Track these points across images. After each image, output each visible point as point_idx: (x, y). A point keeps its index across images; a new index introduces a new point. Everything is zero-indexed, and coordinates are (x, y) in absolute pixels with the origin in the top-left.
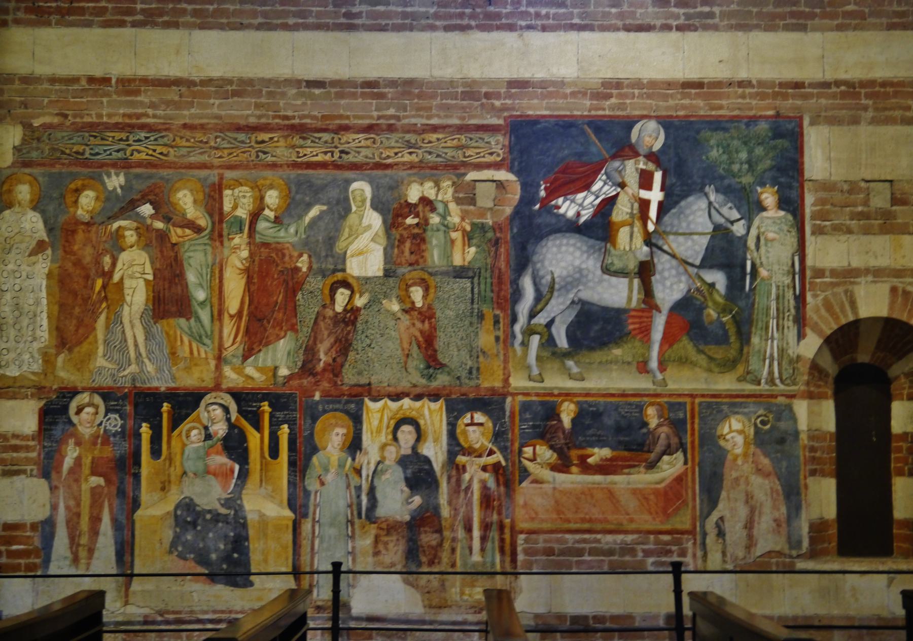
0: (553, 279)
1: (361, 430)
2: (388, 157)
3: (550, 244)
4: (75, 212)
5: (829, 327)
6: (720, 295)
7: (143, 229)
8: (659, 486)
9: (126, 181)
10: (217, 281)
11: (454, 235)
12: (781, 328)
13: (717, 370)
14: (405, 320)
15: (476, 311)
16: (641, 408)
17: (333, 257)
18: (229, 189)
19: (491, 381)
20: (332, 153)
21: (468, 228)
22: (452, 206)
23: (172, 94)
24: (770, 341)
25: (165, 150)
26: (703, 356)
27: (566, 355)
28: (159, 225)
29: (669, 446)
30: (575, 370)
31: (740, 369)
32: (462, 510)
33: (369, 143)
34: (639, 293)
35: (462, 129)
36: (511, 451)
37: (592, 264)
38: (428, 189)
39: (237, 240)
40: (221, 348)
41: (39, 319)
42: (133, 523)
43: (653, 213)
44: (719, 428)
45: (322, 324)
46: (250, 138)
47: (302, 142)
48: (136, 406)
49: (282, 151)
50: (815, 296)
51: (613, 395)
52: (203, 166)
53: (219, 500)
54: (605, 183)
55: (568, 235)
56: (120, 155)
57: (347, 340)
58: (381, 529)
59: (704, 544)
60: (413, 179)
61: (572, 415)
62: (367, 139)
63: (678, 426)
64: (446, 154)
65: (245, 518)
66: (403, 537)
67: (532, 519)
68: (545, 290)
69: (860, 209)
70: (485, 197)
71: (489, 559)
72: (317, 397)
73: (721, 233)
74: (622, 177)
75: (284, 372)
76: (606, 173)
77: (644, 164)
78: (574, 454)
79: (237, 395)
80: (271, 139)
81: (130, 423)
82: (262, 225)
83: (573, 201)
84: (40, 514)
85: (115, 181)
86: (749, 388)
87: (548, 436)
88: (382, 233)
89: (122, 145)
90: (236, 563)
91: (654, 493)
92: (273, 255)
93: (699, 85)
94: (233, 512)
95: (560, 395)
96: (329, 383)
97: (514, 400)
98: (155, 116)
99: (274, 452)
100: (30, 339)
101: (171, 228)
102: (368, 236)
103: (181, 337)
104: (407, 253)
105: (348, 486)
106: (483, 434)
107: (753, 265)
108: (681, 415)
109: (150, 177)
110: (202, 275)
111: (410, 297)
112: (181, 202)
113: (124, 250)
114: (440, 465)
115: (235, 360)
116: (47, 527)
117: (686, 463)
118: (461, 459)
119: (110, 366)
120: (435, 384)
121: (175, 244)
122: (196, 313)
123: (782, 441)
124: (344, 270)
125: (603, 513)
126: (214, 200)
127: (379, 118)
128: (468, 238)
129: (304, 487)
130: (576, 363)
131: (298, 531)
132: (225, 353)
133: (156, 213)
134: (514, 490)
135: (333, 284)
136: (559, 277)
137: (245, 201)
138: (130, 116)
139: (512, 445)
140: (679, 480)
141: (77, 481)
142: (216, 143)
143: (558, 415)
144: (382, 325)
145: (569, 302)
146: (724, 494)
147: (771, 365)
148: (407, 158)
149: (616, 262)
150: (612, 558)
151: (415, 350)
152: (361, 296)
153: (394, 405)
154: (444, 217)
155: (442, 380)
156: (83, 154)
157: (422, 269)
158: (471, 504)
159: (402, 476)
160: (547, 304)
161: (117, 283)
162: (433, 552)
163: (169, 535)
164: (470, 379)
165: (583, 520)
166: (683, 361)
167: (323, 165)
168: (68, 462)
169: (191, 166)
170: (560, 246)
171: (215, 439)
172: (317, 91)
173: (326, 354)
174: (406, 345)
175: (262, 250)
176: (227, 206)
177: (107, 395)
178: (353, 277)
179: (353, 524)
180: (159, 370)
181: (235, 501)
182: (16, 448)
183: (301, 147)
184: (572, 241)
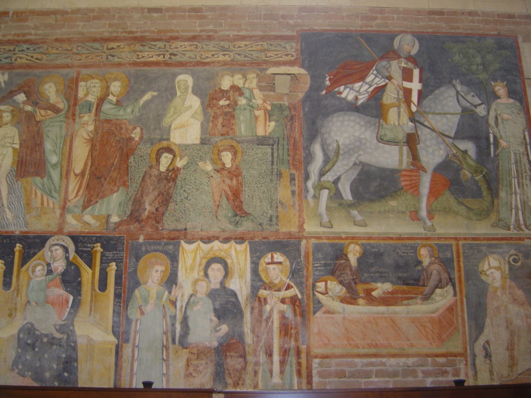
0: (338, 146)
1: (177, 267)
2: (207, 57)
3: (335, 119)
6: (472, 160)
7: (17, 112)
8: (433, 315)
9: (9, 78)
10: (68, 148)
11: (257, 113)
12: (521, 185)
14: (217, 177)
15: (276, 170)
16: (415, 249)
18: (84, 81)
20: (164, 55)
21: (269, 108)
23: (51, 20)
24: (514, 195)
26: (463, 207)
27: (351, 205)
28: (29, 108)
29: (440, 281)
30: (359, 218)
31: (493, 217)
32: (264, 337)
33: (192, 48)
34: (408, 158)
35: (263, 38)
36: (306, 286)
39: (86, 118)
40: (66, 200)
43: (415, 98)
44: (481, 265)
45: (148, 181)
46: (103, 47)
47: (141, 48)
51: (391, 239)
52: (67, 66)
54: (376, 76)
55: (349, 113)
56: (7, 61)
57: (168, 194)
58: (192, 353)
59: (474, 365)
60: (225, 72)
62: (191, 45)
64: (252, 55)
65: (75, 342)
66: (211, 361)
67: (325, 345)
68: (332, 154)
72: (141, 239)
74: (389, 72)
75: (115, 219)
76: (376, 69)
77: (405, 64)
78: (360, 288)
79: (75, 238)
80: (118, 46)
82: (106, 107)
83: (352, 89)
86: (501, 232)
87: (338, 273)
88: (200, 111)
91: (430, 321)
92: (114, 129)
93: (441, 13)
94: (65, 337)
95: (347, 238)
96: (152, 228)
97: (308, 242)
98: (36, 35)
99: (103, 286)
101: (37, 110)
102: (188, 114)
103: (36, 191)
104: (219, 126)
105: (165, 316)
106: (282, 271)
107: (495, 138)
108: (449, 255)
110: (56, 144)
111: (221, 160)
112: (47, 92)
115: (76, 210)
117: (455, 295)
118: (263, 293)
120: (241, 229)
121: (39, 122)
122: (49, 173)
124: (168, 139)
125: (387, 339)
126: (72, 89)
127: (201, 31)
128: (269, 115)
129: (127, 316)
130: (359, 212)
134: (309, 320)
137: (95, 90)
138: (18, 35)
139: (307, 280)
140: (451, 309)
142: (77, 50)
143: (346, 255)
144: (197, 182)
145: (351, 164)
146: (488, 321)
147: (517, 214)
148: (221, 58)
149: (388, 133)
150: (396, 379)
152: (181, 159)
153: (205, 247)
154: (250, 100)
155: (246, 226)
157: (232, 139)
158: (272, 332)
159: (211, 307)
160: (334, 165)
162: (238, 374)
163: (12, 354)
164: (270, 225)
165: (370, 346)
166: (447, 211)
167: (157, 64)
169: (57, 67)
171: (55, 274)
172: (155, 15)
173: (150, 205)
174: (217, 198)
175: (105, 125)
178: (175, 144)
179: (167, 349)
181: (68, 327)
183: (141, 52)
184: (352, 118)
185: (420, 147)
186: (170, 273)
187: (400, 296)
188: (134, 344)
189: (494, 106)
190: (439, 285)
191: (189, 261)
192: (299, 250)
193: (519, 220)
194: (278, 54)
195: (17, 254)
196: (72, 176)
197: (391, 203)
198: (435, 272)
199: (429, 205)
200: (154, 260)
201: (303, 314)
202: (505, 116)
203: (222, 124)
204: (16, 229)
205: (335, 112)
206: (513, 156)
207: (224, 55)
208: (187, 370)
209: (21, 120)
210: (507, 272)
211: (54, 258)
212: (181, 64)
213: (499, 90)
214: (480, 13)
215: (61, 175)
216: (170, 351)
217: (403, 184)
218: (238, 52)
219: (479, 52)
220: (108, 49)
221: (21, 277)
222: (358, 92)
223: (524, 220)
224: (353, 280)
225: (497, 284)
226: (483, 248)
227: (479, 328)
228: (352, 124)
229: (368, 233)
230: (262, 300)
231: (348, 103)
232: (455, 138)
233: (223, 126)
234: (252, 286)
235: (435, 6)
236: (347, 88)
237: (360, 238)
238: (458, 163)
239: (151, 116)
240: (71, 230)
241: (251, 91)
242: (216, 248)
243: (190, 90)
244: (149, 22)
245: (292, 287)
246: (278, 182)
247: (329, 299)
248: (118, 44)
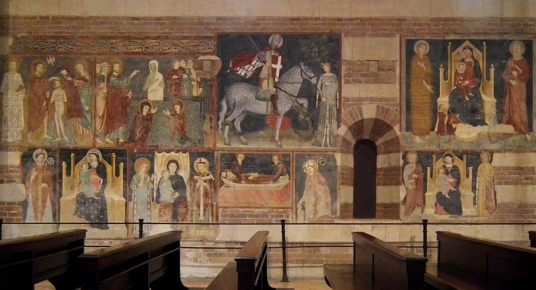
0: (235, 102)
3: (234, 87)
4: (35, 74)
5: (351, 122)
7: (63, 80)
11: (193, 83)
13: (303, 140)
14: (172, 118)
15: (202, 115)
16: (271, 156)
17: (142, 92)
19: (208, 145)
21: (199, 80)
22: (193, 71)
23: (75, 23)
25: (71, 47)
26: (297, 135)
27: (240, 134)
28: (69, 79)
29: (283, 172)
30: (244, 140)
31: (313, 140)
34: (271, 108)
35: (197, 38)
37: (251, 96)
38: (183, 64)
39: (102, 85)
41: (20, 118)
42: (59, 202)
45: (137, 121)
47: (129, 43)
48: (60, 154)
49: (121, 47)
50: (345, 109)
51: (260, 151)
52: (88, 54)
53: (95, 193)
54: (257, 61)
55: (241, 83)
56: (53, 49)
61: (242, 159)
62: (157, 42)
63: (287, 164)
64: (190, 48)
65: (105, 201)
67: (225, 202)
68: (231, 107)
69: (365, 72)
70: (207, 66)
71: (207, 218)
72: (135, 151)
73: (306, 83)
74: (265, 58)
75: (121, 140)
78: (243, 175)
79: (102, 150)
80: (116, 42)
81: (58, 162)
82: (112, 79)
84: (22, 199)
85: (51, 60)
86: (317, 148)
87: (232, 168)
88: (163, 82)
89: (54, 45)
90: (102, 219)
91: (276, 192)
94: (100, 199)
95: (237, 151)
98: (68, 33)
99: (117, 174)
100: (17, 126)
104: (173, 91)
105: (148, 188)
106: (205, 167)
107: (319, 96)
109: (66, 58)
112: (78, 69)
113: (55, 89)
114: (187, 179)
115: (101, 135)
116: (24, 204)
117: (290, 179)
119: (49, 138)
121: (76, 87)
123: (330, 170)
124: (147, 98)
127: (162, 33)
128: (199, 84)
129: (130, 188)
131: (127, 206)
132: (97, 133)
133: (68, 73)
135: (142, 103)
136: (238, 101)
137: (105, 68)
138: (57, 33)
139: (217, 171)
140: (287, 186)
141: (36, 185)
142: (93, 44)
147: (326, 138)
148: (174, 50)
151: (176, 132)
152: (154, 109)
153: (167, 155)
154: (189, 75)
155: (188, 144)
156: (38, 49)
157: (180, 97)
159: (171, 184)
160: (232, 112)
161: (52, 103)
163: (74, 207)
164: (199, 144)
165: (246, 203)
166: (289, 137)
167: (138, 53)
168: (33, 177)
170: (238, 88)
172: (136, 22)
174: (173, 129)
175: (112, 89)
176: (98, 71)
177: (48, 150)
179: (150, 204)
180: (70, 139)
182: (11, 171)
184: (243, 86)
186: (151, 168)
187: (262, 179)
188: (134, 202)
189: (321, 78)
190: (282, 174)
191: (160, 162)
193: (327, 142)
194: (204, 48)
195: (72, 159)
196: (98, 118)
197: (260, 132)
198: (280, 168)
200: (142, 161)
201: (215, 188)
202: (327, 84)
203: (175, 89)
204: (71, 145)
205: (234, 83)
206: (328, 107)
207: (175, 48)
208: (159, 214)
209: (66, 86)
210: (317, 169)
211: (92, 160)
212: (151, 54)
213: (326, 68)
214: (321, 19)
215: (91, 117)
216: (152, 205)
217: (268, 122)
218: (183, 47)
219: (317, 44)
220: (110, 44)
221: (76, 170)
222: (247, 70)
223: (330, 142)
224: (240, 171)
225: (311, 174)
226: (306, 156)
227: (300, 196)
228: (243, 89)
229: (248, 148)
230: (195, 181)
231: (242, 77)
232: (298, 97)
233: (176, 91)
234: (191, 174)
235: (295, 15)
236: (241, 68)
237: (244, 151)
238: (298, 111)
239: (137, 84)
240: (99, 146)
241: (190, 71)
242: (172, 155)
243: (157, 70)
244: (132, 26)
245: (210, 175)
246: (204, 121)
247: (228, 180)
248: (116, 41)
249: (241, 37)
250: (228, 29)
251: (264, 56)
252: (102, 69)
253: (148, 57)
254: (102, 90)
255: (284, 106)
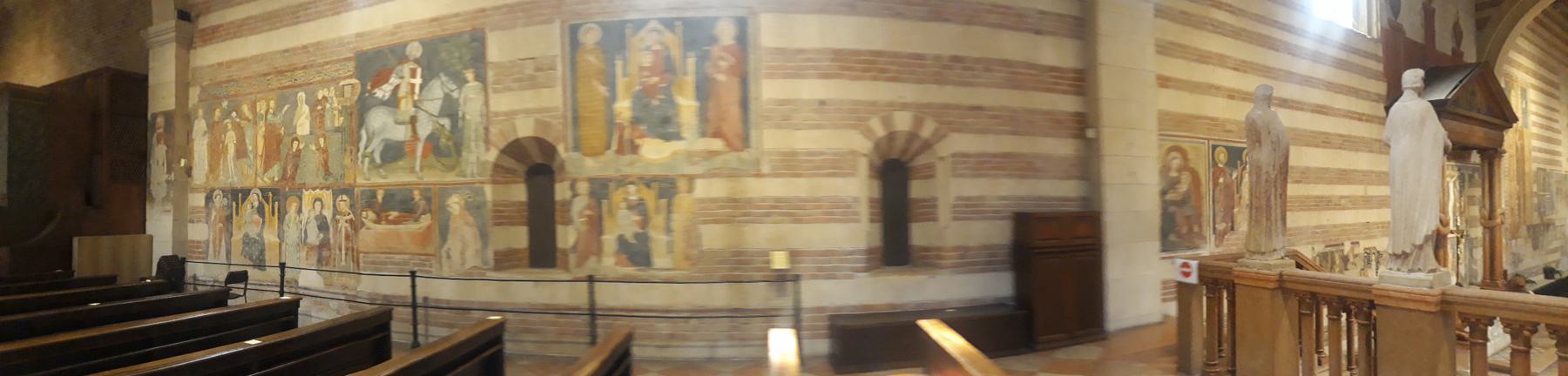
7: (233, 123)
16: (411, 191)
21: (340, 108)
22: (334, 98)
27: (380, 166)
28: (238, 120)
29: (424, 210)
30: (384, 173)
37: (390, 120)
51: (398, 185)
63: (428, 200)
68: (371, 135)
75: (276, 179)
78: (383, 214)
82: (269, 116)
106: (346, 205)
120: (328, 183)
140: (429, 227)
155: (331, 180)
185: (418, 124)
190: (424, 213)
192: (354, 194)
199: (421, 162)
217: (407, 150)
241: (332, 98)
249: (378, 53)
250: (367, 46)
251: (401, 71)
252: (261, 107)
253: (297, 90)
254: (262, 130)
255: (424, 130)
